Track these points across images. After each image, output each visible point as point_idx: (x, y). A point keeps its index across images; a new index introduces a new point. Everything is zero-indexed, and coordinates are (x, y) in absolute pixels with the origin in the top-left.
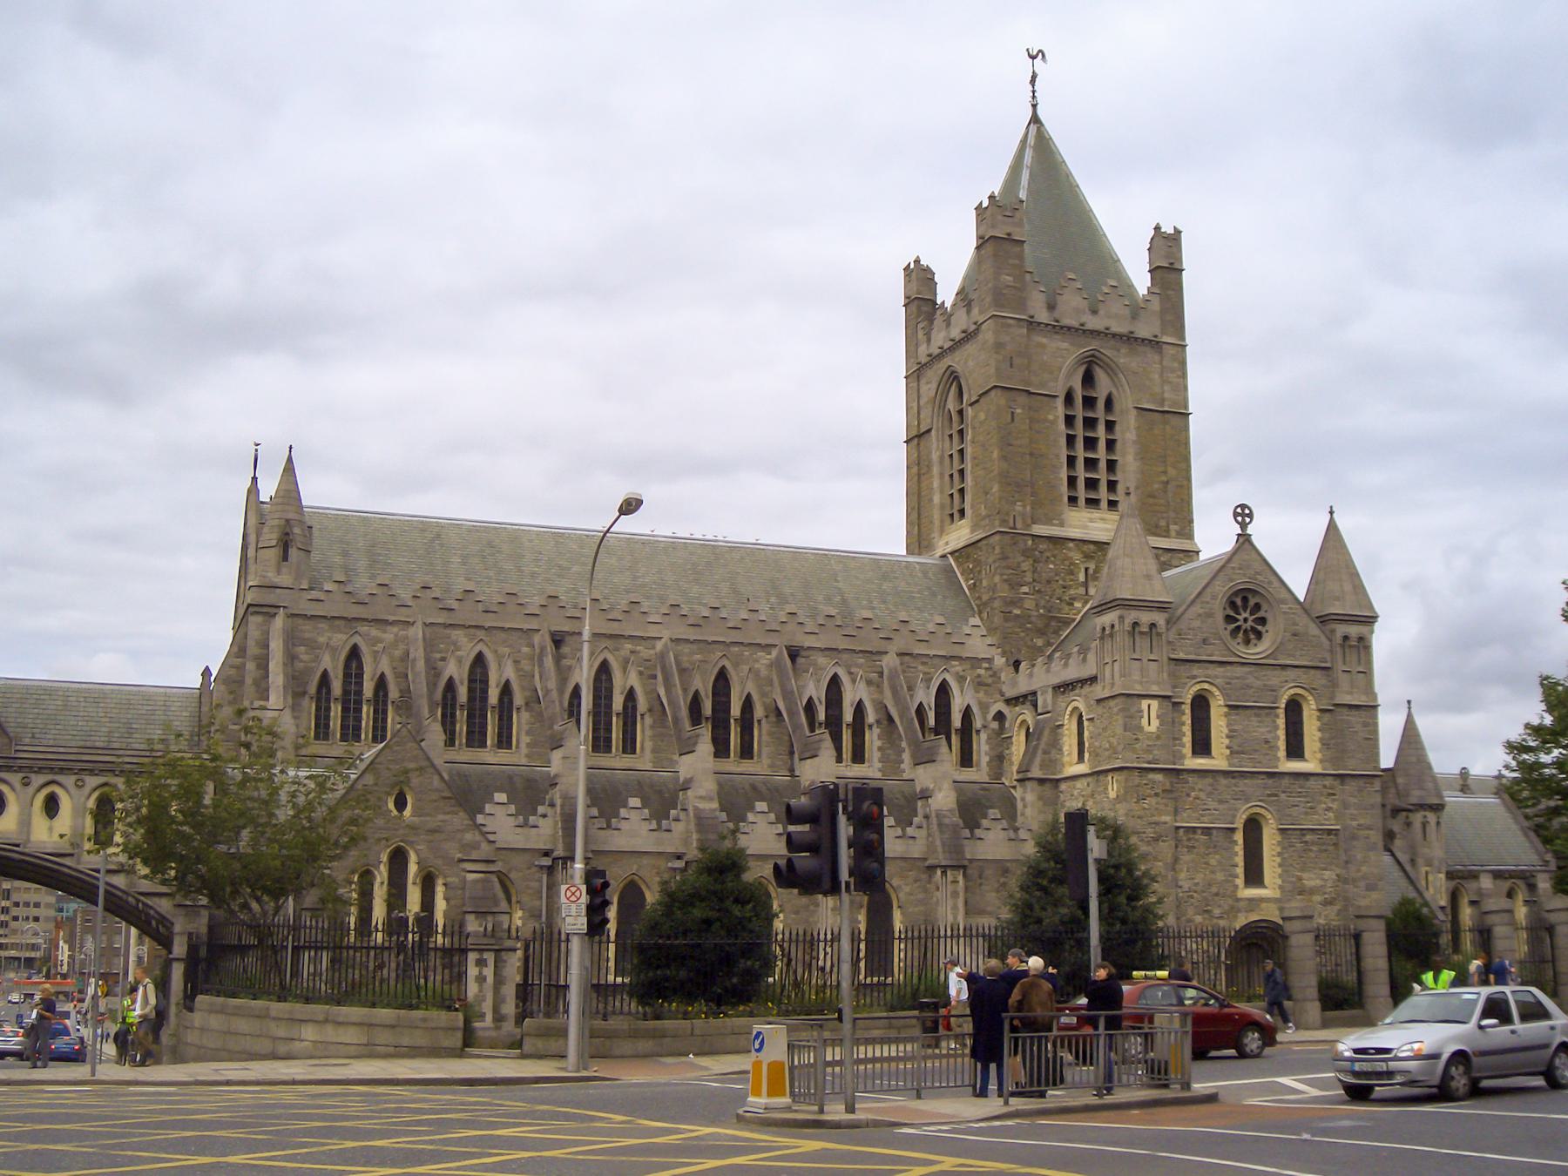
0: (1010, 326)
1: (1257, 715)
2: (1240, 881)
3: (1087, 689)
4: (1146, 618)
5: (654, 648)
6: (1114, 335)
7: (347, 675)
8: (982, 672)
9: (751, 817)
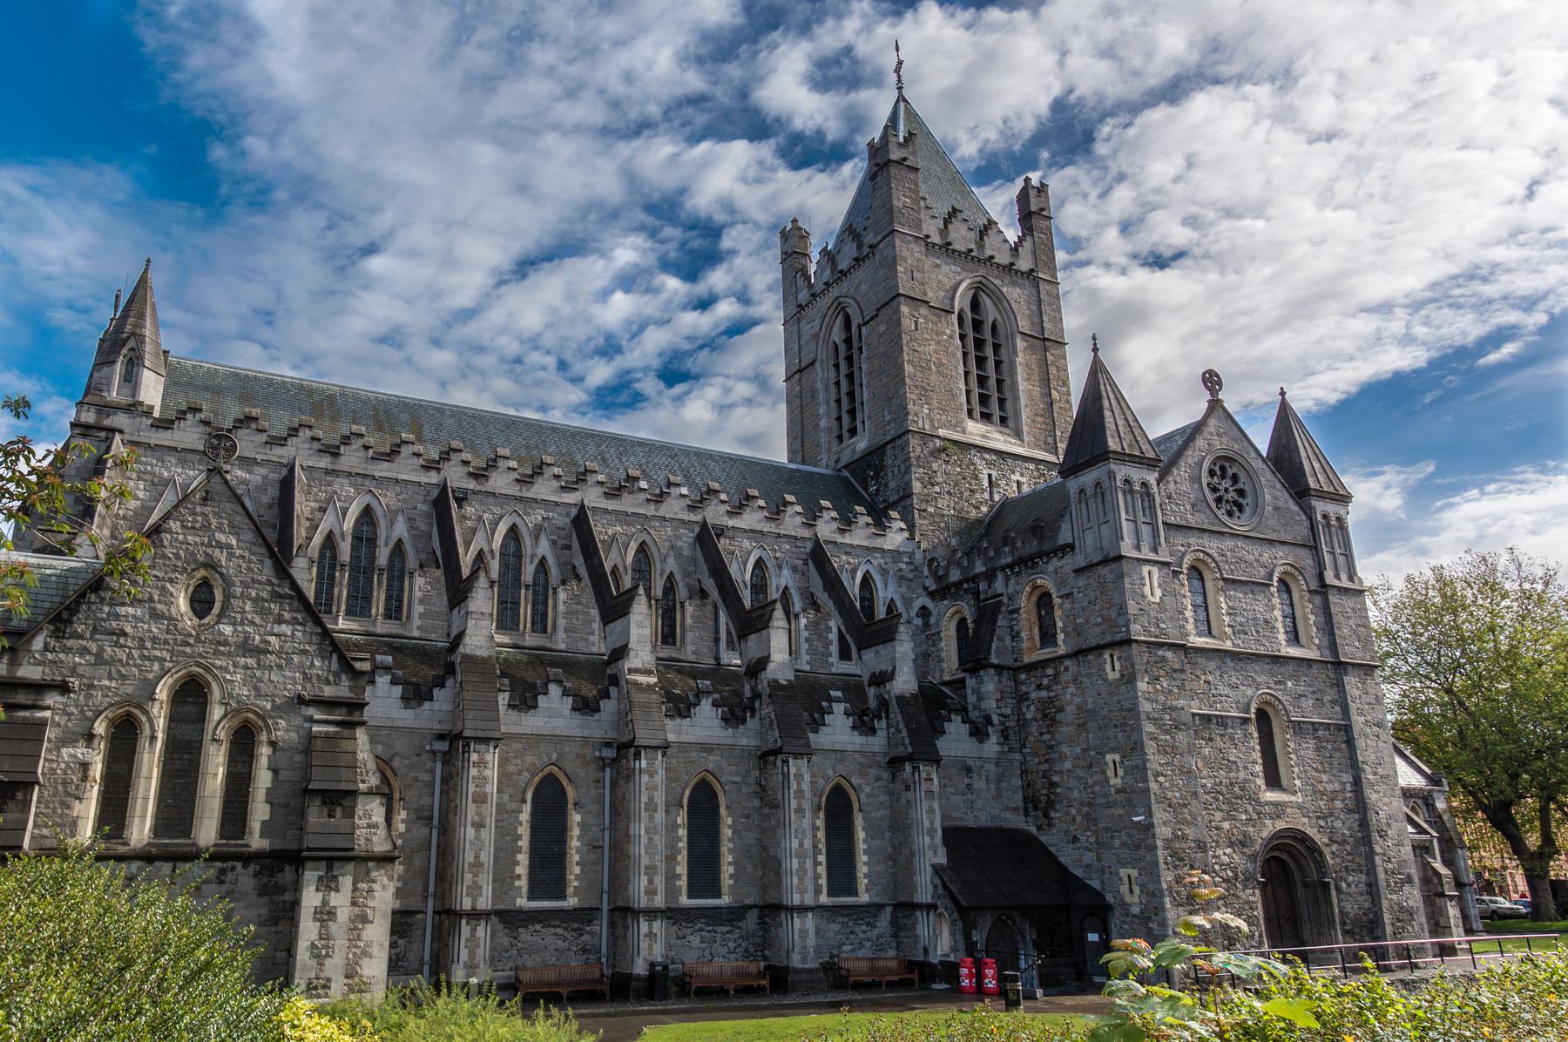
0: (910, 242)
1: (1253, 592)
2: (1260, 782)
3: (1055, 563)
6: (998, 266)
8: (903, 566)
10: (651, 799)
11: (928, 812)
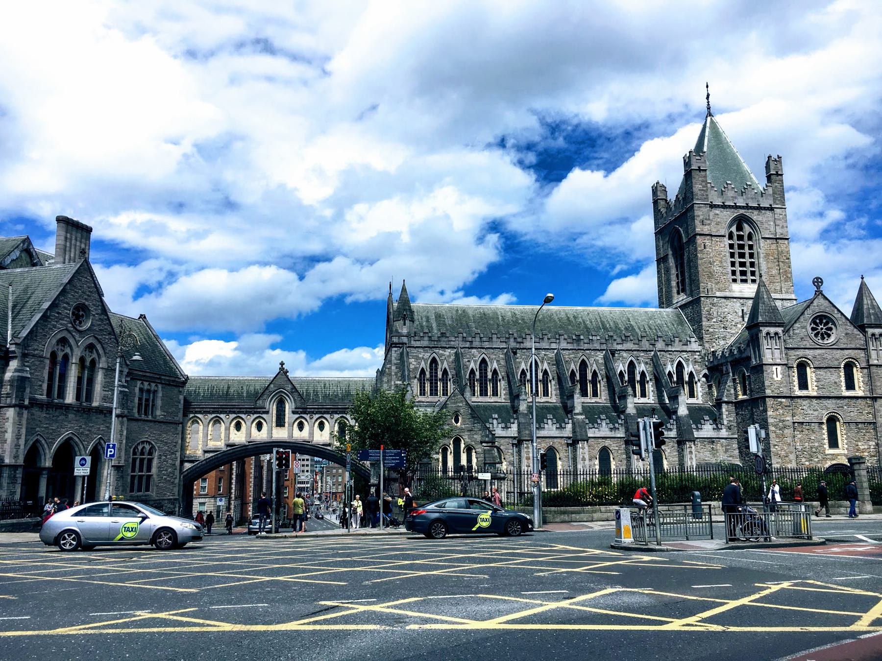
1: (830, 372)
2: (827, 446)
4: (772, 330)
5: (554, 353)
7: (431, 369)
8: (697, 357)
9: (599, 421)
10: (583, 457)
11: (690, 459)
